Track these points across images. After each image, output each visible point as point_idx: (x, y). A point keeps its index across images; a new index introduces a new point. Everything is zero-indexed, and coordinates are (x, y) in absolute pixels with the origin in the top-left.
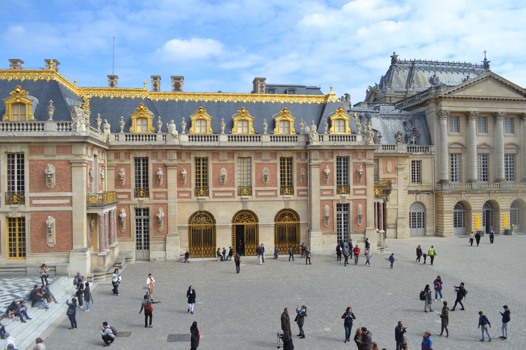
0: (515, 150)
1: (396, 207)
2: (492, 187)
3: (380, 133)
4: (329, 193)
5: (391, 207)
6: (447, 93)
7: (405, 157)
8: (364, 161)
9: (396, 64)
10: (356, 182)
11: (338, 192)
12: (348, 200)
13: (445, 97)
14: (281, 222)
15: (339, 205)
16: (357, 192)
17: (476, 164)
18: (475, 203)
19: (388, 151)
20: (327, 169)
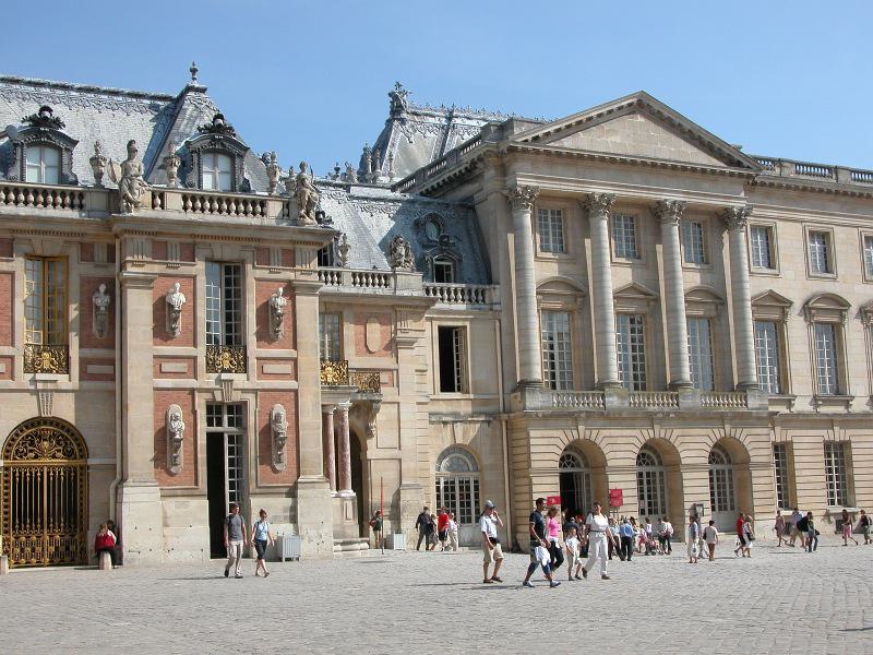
0: (713, 307)
1: (395, 453)
2: (656, 403)
3: (345, 237)
4: (181, 366)
6: (529, 138)
7: (417, 308)
8: (291, 275)
9: (404, 115)
10: (267, 335)
11: (211, 367)
12: (244, 391)
13: (525, 151)
14: (25, 461)
15: (214, 410)
16: (269, 368)
17: (612, 337)
18: (615, 447)
19: (369, 290)
20: (175, 292)
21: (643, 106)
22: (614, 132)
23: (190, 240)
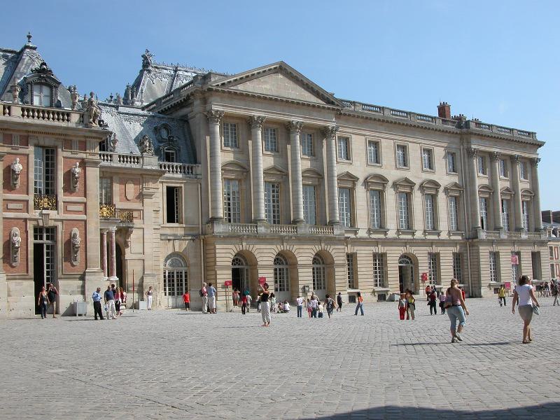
0: (317, 180)
1: (141, 256)
2: (285, 231)
3: (115, 135)
4: (19, 206)
5: (134, 257)
6: (220, 84)
7: (155, 176)
8: (84, 156)
9: (150, 68)
10: (69, 189)
11: (37, 206)
12: (56, 220)
13: (217, 91)
15: (38, 231)
16: (70, 208)
17: (262, 195)
18: (263, 255)
19: (128, 165)
20: (16, 163)
21: (282, 69)
22: (265, 82)
23: (26, 134)
